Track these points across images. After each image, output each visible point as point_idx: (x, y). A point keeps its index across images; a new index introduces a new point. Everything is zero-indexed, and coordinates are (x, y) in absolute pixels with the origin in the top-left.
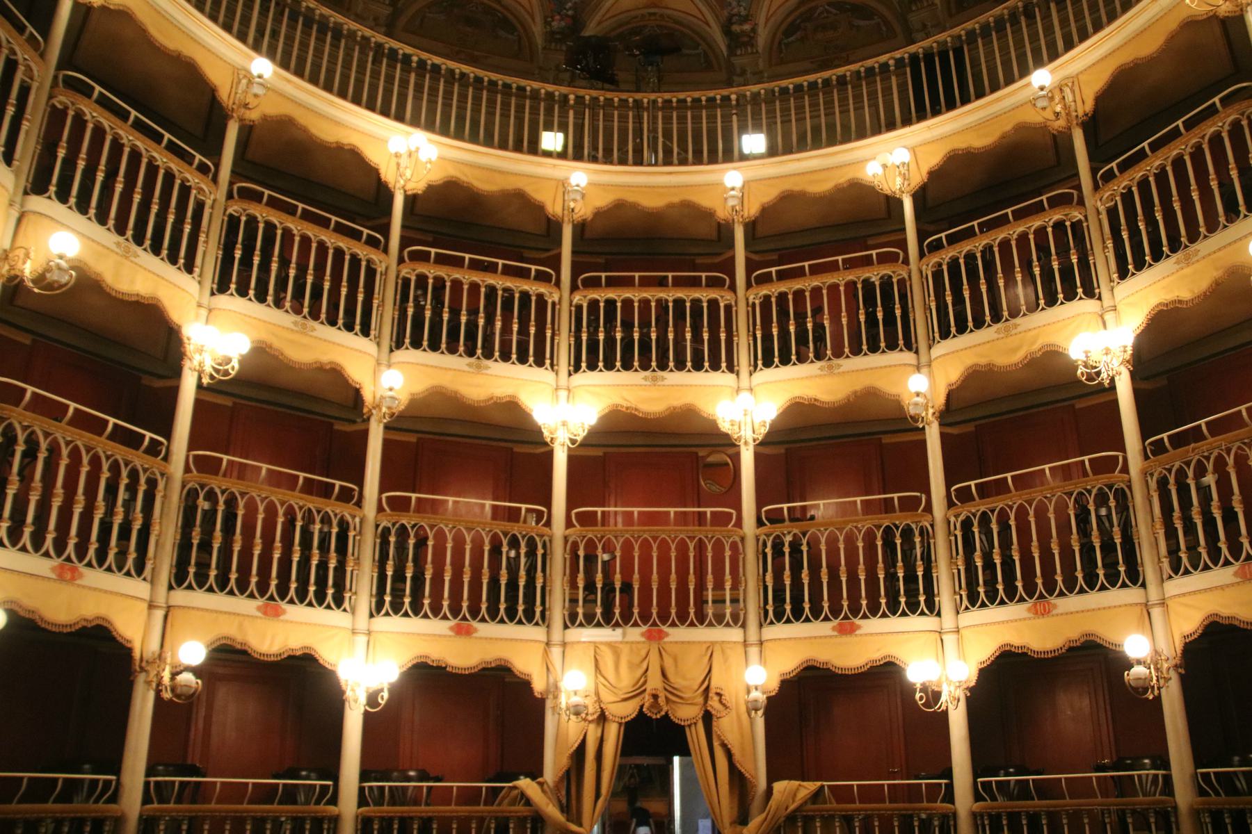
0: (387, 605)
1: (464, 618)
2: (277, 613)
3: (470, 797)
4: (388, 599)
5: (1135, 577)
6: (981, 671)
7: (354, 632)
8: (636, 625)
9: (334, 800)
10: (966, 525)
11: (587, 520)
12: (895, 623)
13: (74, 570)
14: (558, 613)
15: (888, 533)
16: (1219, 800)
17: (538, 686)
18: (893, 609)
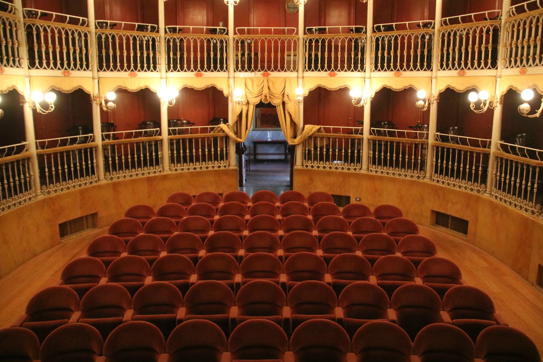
0: (172, 68)
1: (199, 71)
2: (135, 75)
3: (204, 131)
4: (172, 66)
5: (429, 67)
6: (377, 94)
7: (161, 78)
8: (259, 71)
9: (160, 134)
10: (377, 40)
11: (242, 32)
12: (349, 74)
13: (68, 72)
14: (232, 66)
15: (350, 40)
16: (440, 143)
17: (226, 93)
18: (349, 68)
